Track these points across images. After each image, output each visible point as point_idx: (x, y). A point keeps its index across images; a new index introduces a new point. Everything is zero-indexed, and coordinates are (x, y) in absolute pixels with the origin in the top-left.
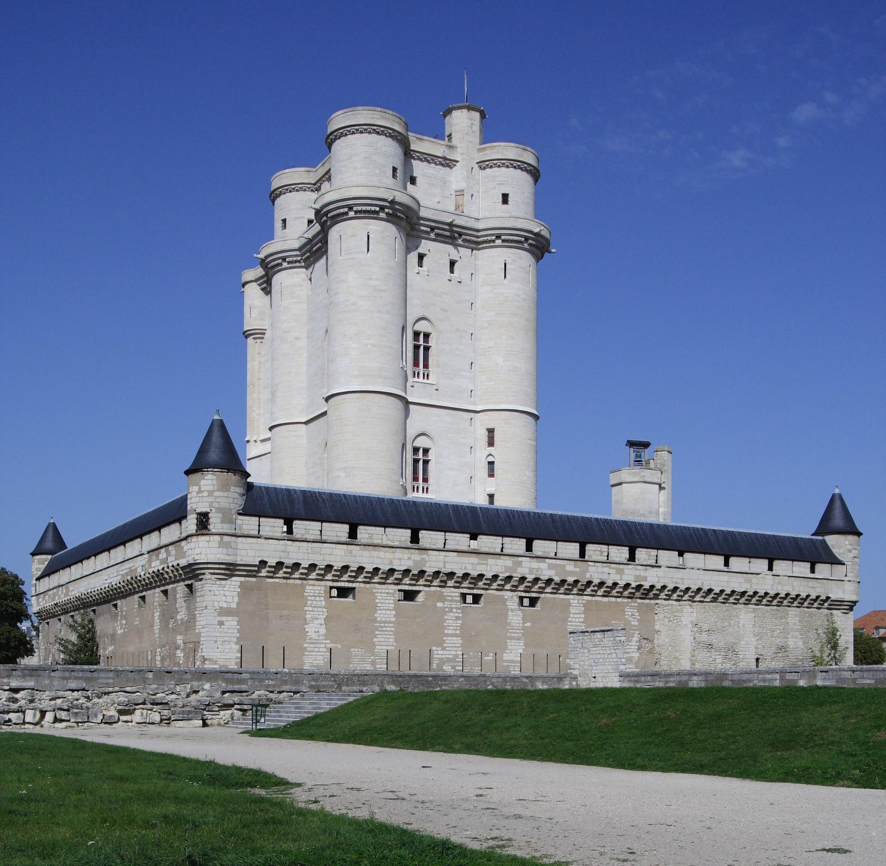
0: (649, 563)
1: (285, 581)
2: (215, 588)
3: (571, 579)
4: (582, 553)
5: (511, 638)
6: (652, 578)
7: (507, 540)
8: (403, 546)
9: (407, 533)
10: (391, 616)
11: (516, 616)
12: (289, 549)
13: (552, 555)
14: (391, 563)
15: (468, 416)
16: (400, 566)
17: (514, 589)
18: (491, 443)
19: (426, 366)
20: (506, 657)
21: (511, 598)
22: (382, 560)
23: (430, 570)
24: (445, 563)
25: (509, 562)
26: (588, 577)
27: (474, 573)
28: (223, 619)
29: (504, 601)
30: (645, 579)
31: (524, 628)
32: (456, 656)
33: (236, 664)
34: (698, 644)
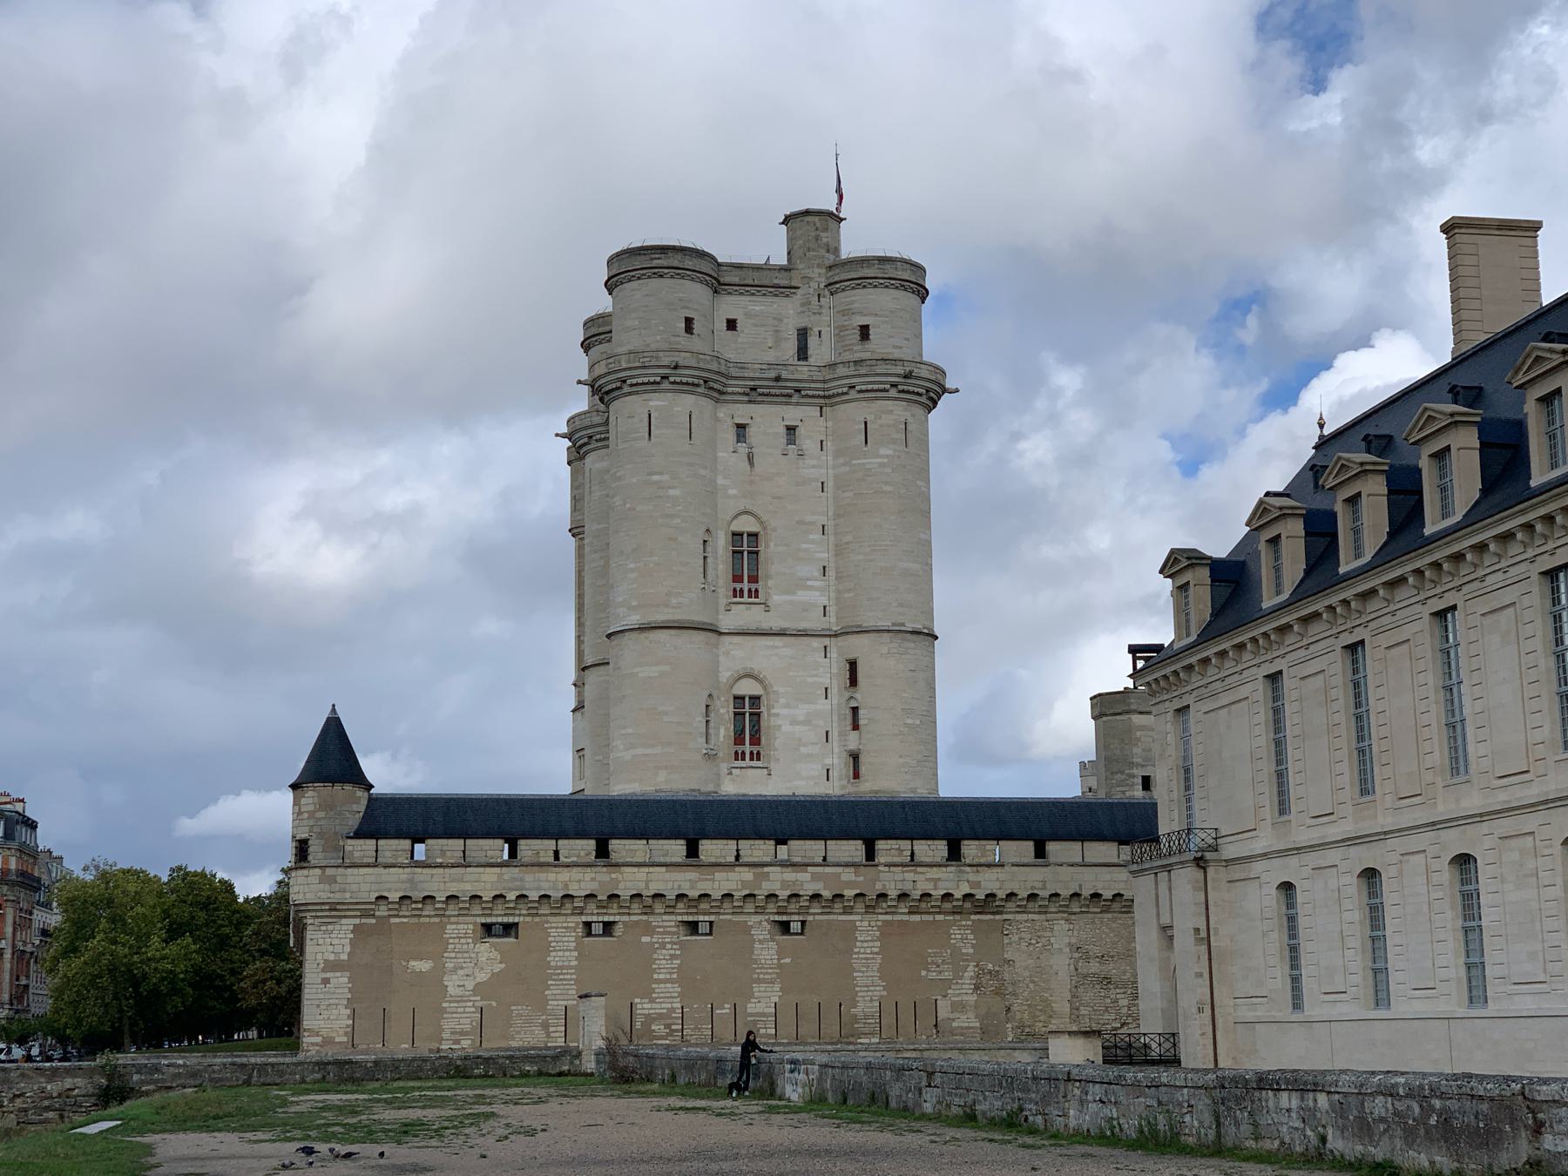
0: (982, 861)
1: (415, 920)
2: (319, 935)
3: (849, 893)
4: (870, 854)
5: (759, 981)
6: (990, 882)
7: (744, 844)
8: (580, 861)
9: (591, 844)
10: (571, 958)
11: (767, 950)
12: (418, 878)
13: (820, 860)
14: (566, 886)
15: (817, 643)
16: (578, 890)
17: (760, 911)
18: (853, 681)
19: (754, 579)
20: (751, 1008)
21: (760, 926)
22: (554, 882)
23: (625, 894)
24: (647, 882)
25: (747, 875)
26: (879, 887)
27: (694, 894)
28: (328, 975)
29: (746, 929)
30: (977, 885)
31: (780, 966)
32: (673, 1010)
33: (346, 1034)
34: (1081, 979)
